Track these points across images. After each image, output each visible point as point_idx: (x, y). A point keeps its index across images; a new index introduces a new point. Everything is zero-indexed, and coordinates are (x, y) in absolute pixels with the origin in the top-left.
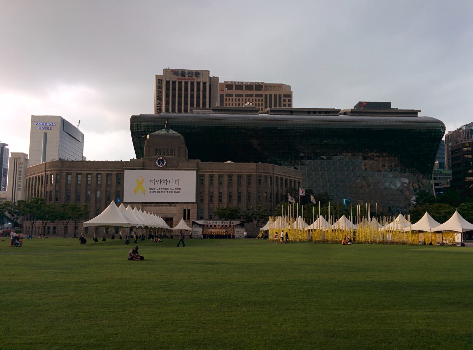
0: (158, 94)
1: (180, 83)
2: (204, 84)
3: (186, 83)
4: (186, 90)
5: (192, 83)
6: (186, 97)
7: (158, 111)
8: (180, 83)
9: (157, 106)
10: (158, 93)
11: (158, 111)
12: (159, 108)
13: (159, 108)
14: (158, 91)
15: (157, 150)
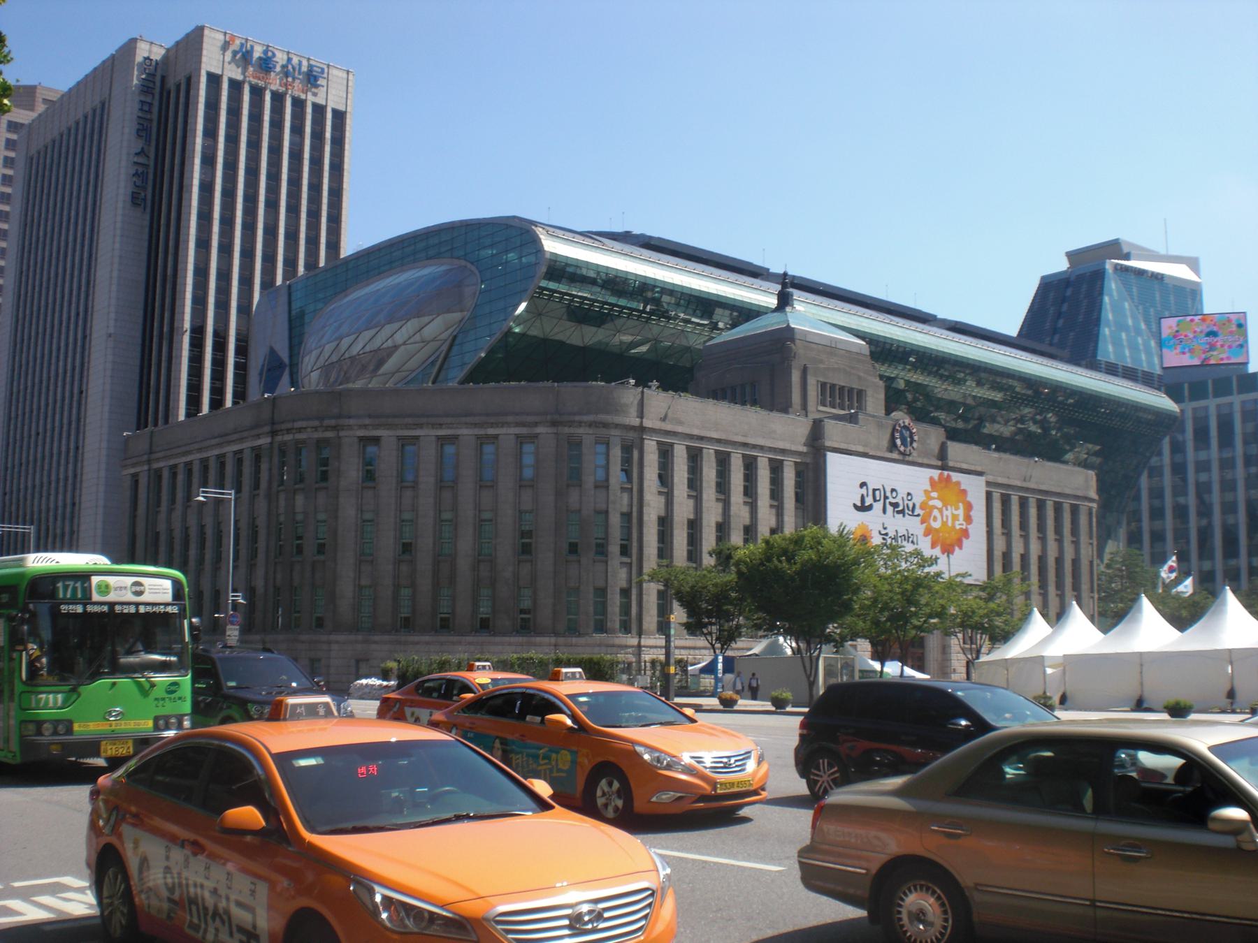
0: (140, 114)
1: (257, 92)
2: (339, 116)
3: (278, 98)
4: (277, 124)
5: (299, 104)
6: (275, 151)
7: (139, 183)
8: (257, 92)
9: (136, 163)
10: (141, 110)
11: (139, 183)
12: (140, 170)
13: (143, 173)
14: (142, 102)
15: (823, 385)
